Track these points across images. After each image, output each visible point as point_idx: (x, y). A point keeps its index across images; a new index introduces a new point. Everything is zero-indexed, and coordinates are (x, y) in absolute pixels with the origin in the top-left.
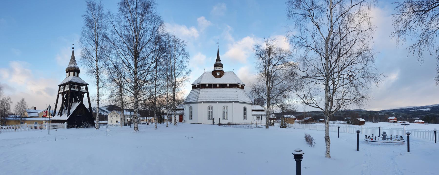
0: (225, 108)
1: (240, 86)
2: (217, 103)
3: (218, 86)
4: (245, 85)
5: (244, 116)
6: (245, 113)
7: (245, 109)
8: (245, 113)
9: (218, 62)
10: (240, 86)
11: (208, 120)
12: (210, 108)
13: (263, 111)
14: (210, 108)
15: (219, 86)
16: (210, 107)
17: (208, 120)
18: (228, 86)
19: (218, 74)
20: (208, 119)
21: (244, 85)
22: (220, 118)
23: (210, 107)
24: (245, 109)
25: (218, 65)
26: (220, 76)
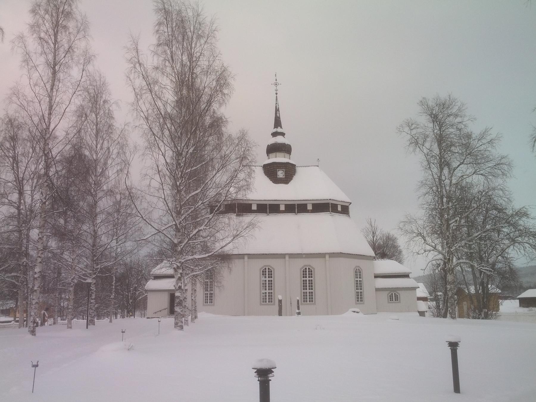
1: (339, 209)
2: (285, 258)
5: (357, 292)
6: (359, 285)
7: (358, 273)
8: (359, 285)
9: (279, 140)
10: (339, 209)
11: (261, 304)
14: (268, 272)
17: (261, 304)
18: (310, 207)
19: (281, 174)
20: (261, 303)
21: (347, 204)
24: (358, 273)
26: (287, 180)
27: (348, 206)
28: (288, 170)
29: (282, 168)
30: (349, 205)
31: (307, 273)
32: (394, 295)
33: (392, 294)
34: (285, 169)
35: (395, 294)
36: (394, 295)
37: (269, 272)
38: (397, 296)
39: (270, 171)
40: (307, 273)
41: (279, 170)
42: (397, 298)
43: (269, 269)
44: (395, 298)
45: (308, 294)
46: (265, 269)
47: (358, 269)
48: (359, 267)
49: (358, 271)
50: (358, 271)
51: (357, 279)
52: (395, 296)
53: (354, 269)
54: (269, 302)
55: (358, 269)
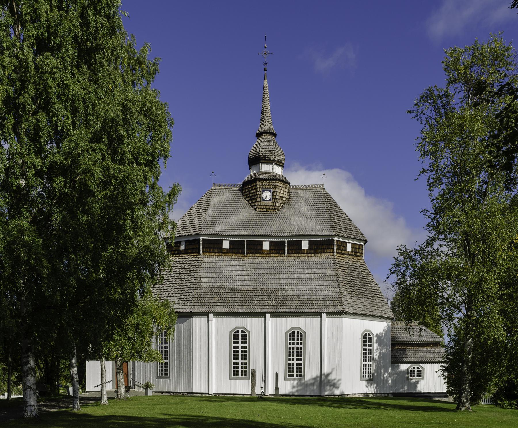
0: (294, 336)
1: (349, 248)
3: (268, 248)
4: (366, 242)
10: (349, 248)
11: (231, 378)
12: (240, 337)
13: (437, 344)
15: (270, 245)
16: (240, 333)
17: (231, 378)
19: (267, 195)
21: (362, 243)
22: (277, 374)
23: (240, 333)
25: (265, 156)
27: (362, 245)
28: (277, 190)
29: (268, 187)
30: (365, 244)
31: (296, 338)
32: (416, 370)
33: (414, 368)
34: (273, 188)
35: (418, 368)
36: (416, 370)
37: (242, 335)
38: (421, 371)
39: (252, 192)
40: (296, 338)
41: (264, 191)
42: (420, 374)
43: (242, 331)
44: (418, 374)
45: (295, 366)
46: (238, 331)
47: (367, 333)
48: (370, 331)
49: (368, 336)
50: (368, 336)
51: (365, 347)
52: (418, 371)
53: (362, 334)
54: (242, 375)
55: (367, 333)
